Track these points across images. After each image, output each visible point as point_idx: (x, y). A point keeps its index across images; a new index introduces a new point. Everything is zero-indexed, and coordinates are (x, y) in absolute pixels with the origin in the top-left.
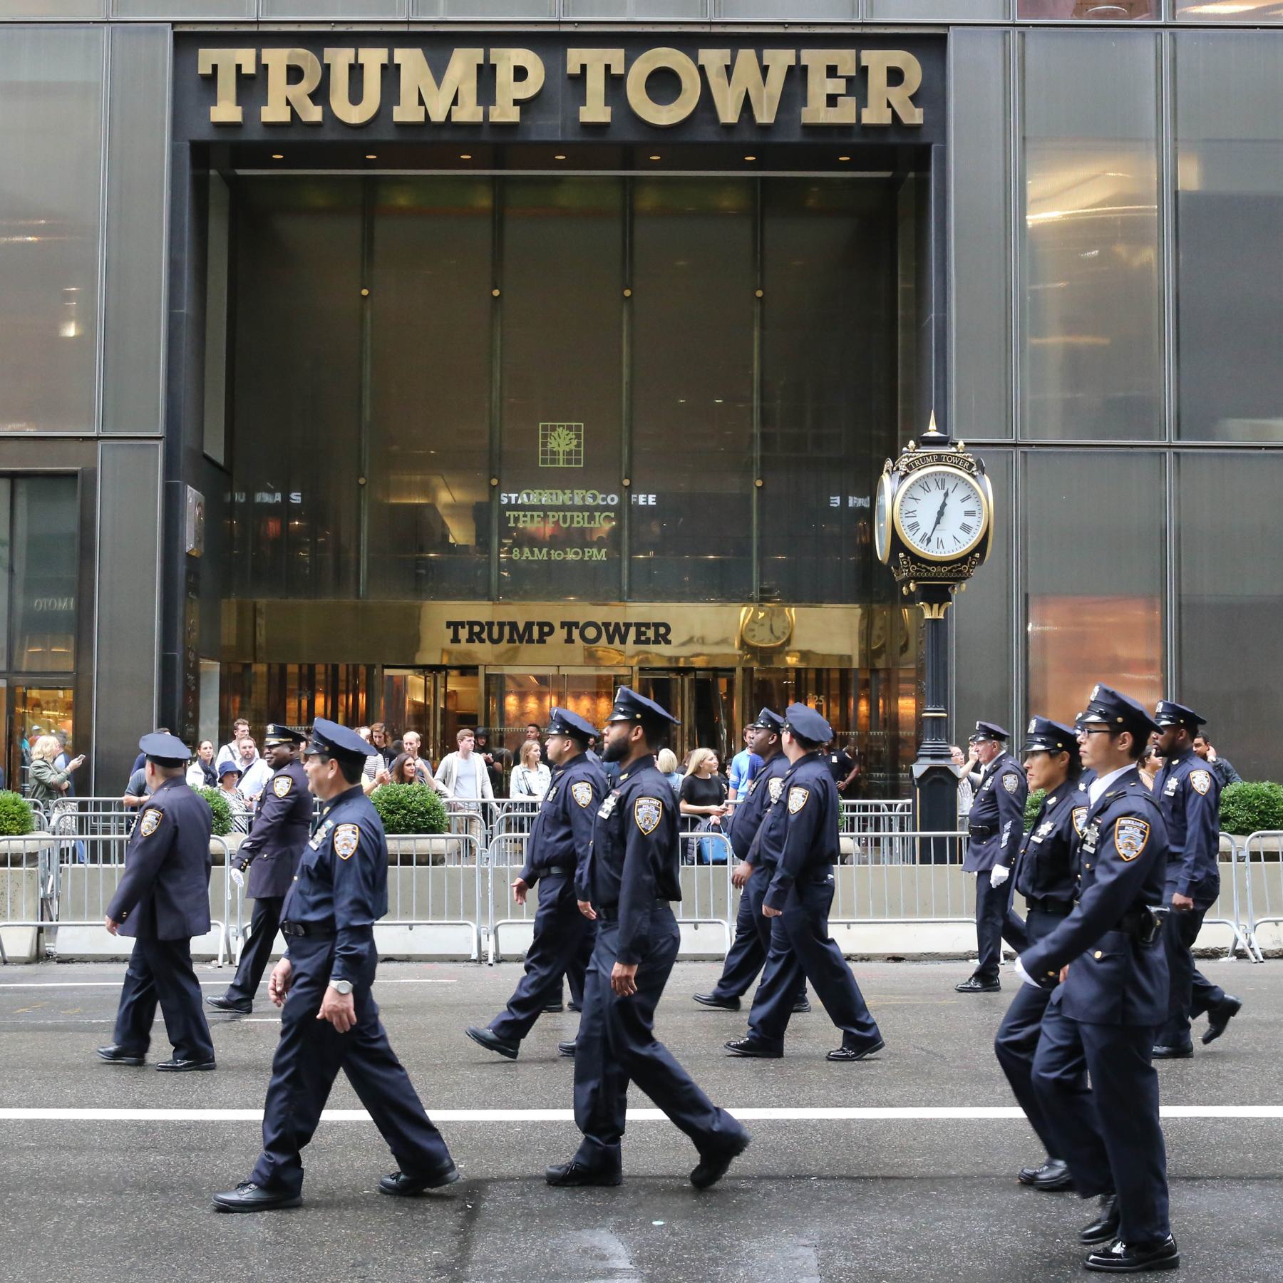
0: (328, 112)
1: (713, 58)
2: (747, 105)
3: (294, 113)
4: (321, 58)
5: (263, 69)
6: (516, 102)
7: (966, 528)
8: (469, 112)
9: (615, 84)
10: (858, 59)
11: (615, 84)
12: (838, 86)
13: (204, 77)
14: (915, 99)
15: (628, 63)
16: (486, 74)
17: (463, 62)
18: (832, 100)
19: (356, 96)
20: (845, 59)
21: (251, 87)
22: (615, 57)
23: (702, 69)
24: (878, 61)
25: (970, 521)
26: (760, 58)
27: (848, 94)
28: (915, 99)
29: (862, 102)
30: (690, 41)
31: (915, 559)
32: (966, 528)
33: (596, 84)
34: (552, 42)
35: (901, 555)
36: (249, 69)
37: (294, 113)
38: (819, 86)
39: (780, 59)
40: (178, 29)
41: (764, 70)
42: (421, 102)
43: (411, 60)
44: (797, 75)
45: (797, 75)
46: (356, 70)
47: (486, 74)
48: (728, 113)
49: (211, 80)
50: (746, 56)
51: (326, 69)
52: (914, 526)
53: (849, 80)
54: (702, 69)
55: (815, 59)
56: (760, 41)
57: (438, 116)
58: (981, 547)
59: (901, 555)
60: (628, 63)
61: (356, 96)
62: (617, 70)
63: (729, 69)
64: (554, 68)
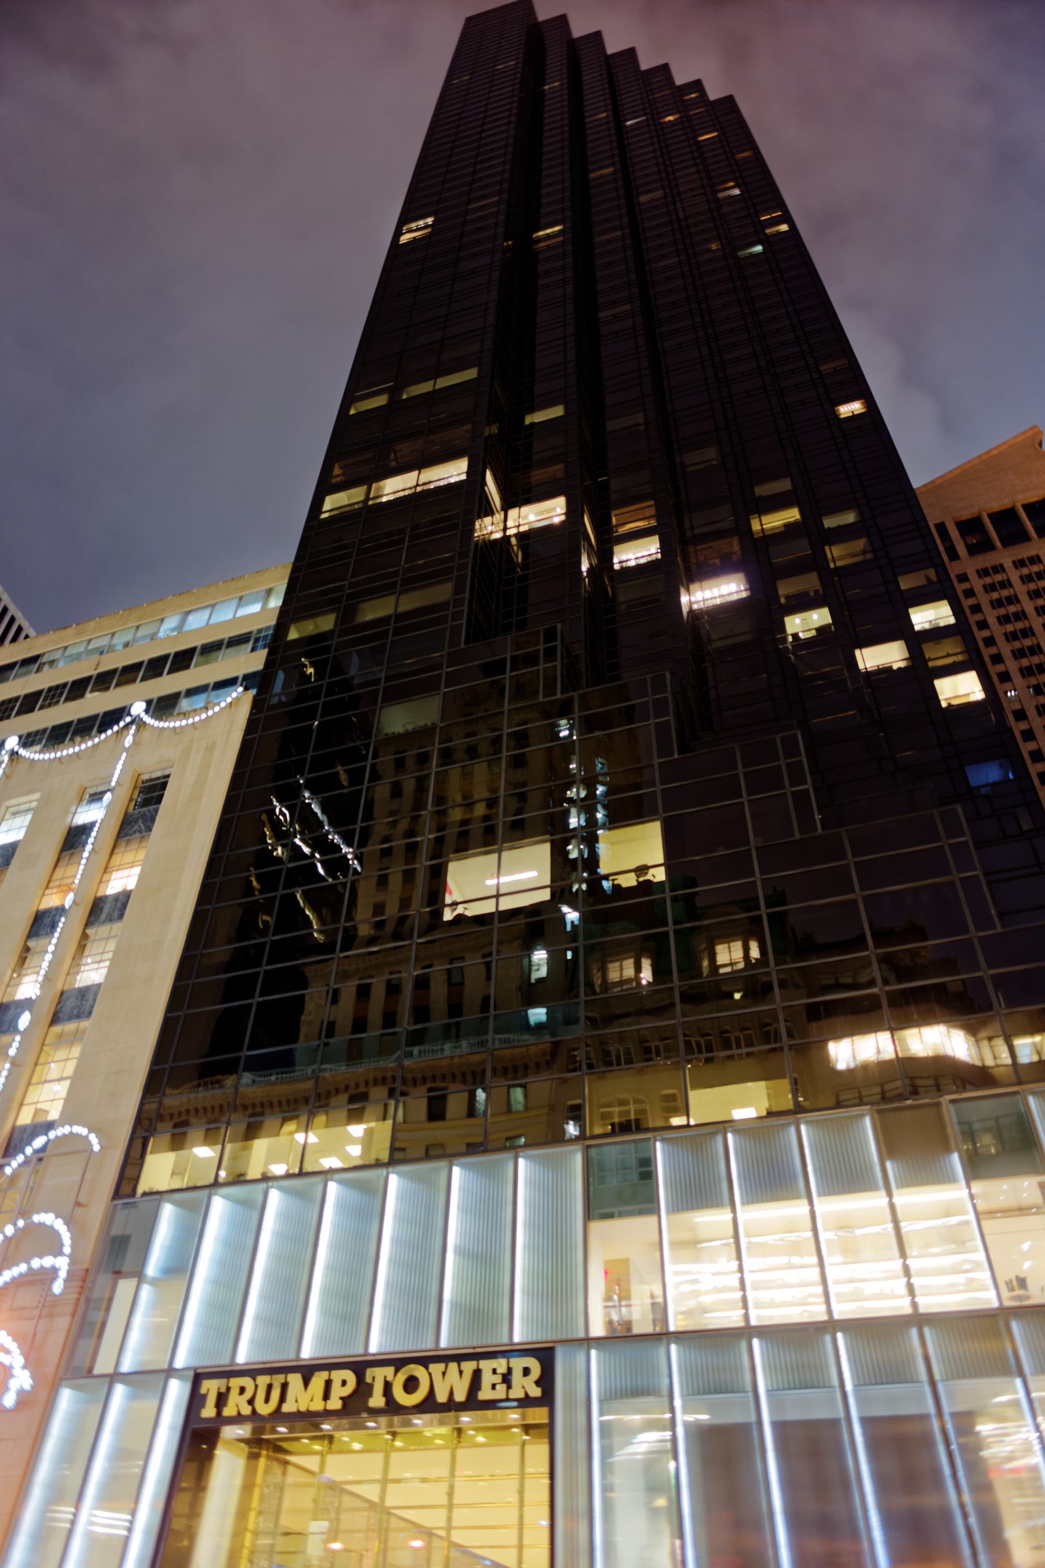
0: (254, 1411)
1: (436, 1368)
2: (451, 1393)
4: (254, 1380)
6: (341, 1398)
8: (318, 1405)
9: (388, 1386)
11: (388, 1386)
12: (498, 1379)
14: (538, 1383)
16: (328, 1384)
17: (318, 1381)
18: (494, 1387)
19: (267, 1400)
20: (501, 1364)
21: (222, 1399)
22: (389, 1371)
23: (430, 1374)
24: (518, 1364)
26: (459, 1366)
28: (538, 1383)
29: (509, 1387)
30: (424, 1361)
33: (378, 1389)
34: (359, 1367)
36: (223, 1390)
38: (487, 1379)
39: (469, 1367)
41: (461, 1372)
43: (295, 1380)
44: (477, 1374)
45: (477, 1374)
46: (270, 1387)
47: (328, 1384)
48: (442, 1397)
50: (453, 1366)
51: (256, 1386)
54: (430, 1374)
55: (486, 1365)
57: (303, 1409)
61: (267, 1400)
62: (390, 1378)
63: (444, 1374)
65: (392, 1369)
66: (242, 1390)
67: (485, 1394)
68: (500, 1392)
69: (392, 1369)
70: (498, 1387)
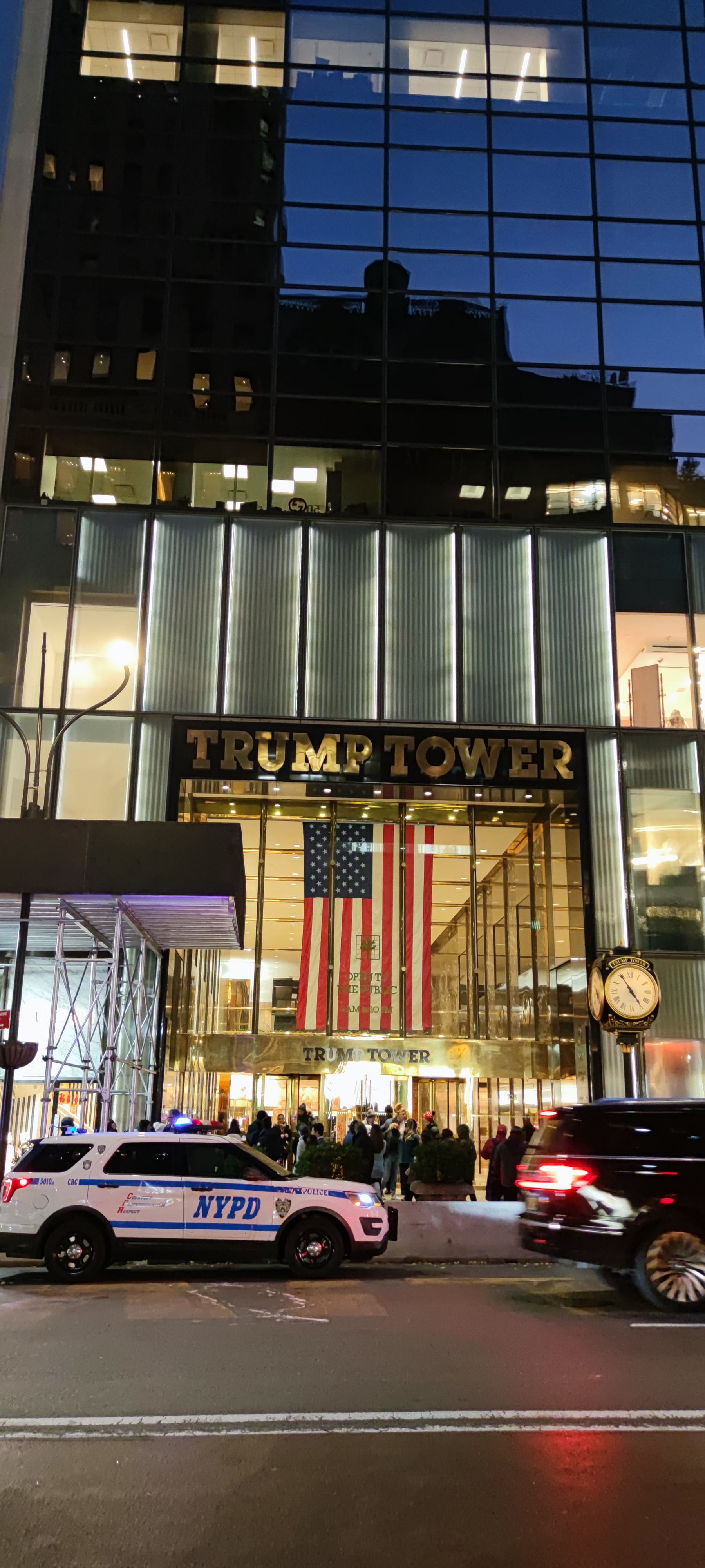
3: (238, 765)
5: (222, 742)
7: (646, 1000)
8: (333, 767)
10: (538, 744)
12: (528, 758)
13: (190, 744)
14: (569, 766)
15: (417, 744)
18: (525, 766)
25: (647, 996)
27: (533, 763)
28: (569, 766)
29: (541, 767)
31: (618, 1017)
32: (646, 1000)
35: (610, 1015)
36: (215, 741)
37: (238, 765)
39: (496, 744)
40: (176, 718)
42: (307, 761)
49: (194, 746)
52: (617, 999)
53: (534, 756)
56: (486, 735)
58: (655, 1012)
59: (610, 1015)
60: (417, 744)
62: (411, 747)
64: (378, 745)
65: (412, 738)
66: (239, 745)
67: (515, 771)
68: (531, 773)
69: (412, 738)
70: (529, 765)
